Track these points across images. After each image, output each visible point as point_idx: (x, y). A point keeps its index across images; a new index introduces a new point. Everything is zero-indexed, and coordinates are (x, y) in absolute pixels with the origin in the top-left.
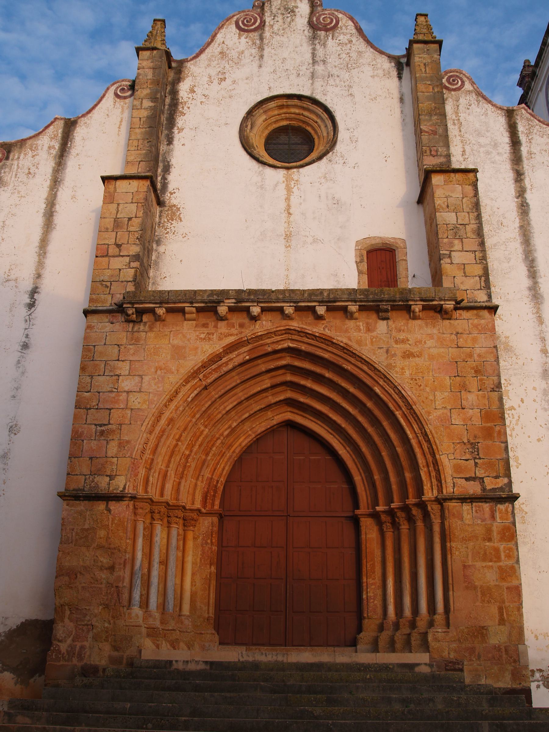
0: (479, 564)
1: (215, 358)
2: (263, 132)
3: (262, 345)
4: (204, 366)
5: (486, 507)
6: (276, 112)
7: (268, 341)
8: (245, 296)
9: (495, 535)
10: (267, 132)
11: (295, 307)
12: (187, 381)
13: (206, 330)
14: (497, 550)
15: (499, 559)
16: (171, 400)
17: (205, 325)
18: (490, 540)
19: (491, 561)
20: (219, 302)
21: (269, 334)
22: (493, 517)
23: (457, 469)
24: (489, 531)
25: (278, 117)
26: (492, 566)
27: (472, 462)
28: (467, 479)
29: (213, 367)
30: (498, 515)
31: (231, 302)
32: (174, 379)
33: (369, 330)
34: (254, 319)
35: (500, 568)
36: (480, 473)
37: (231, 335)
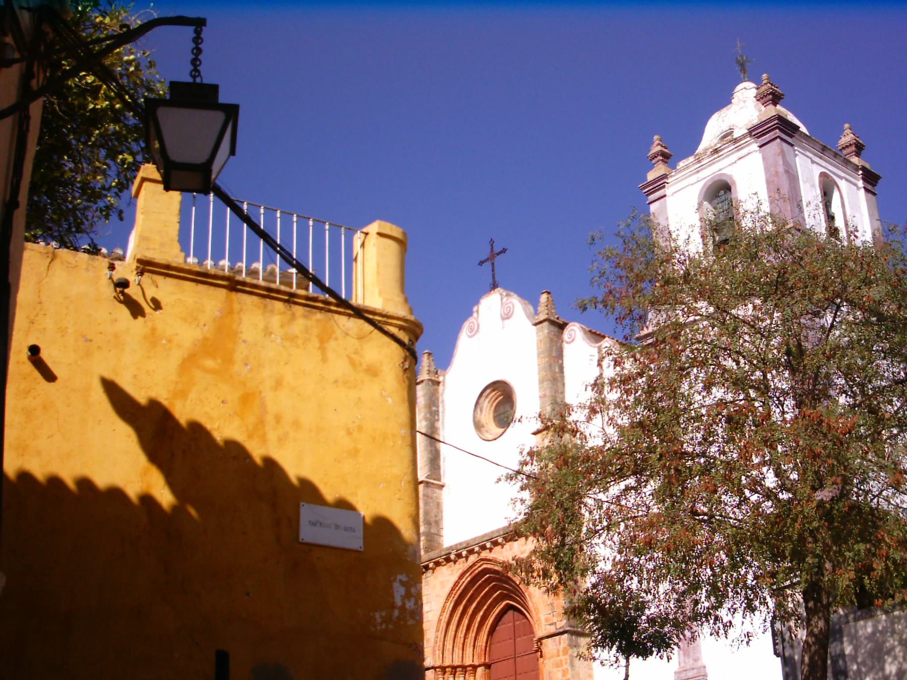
0: (555, 670)
1: (456, 584)
2: (490, 410)
3: (475, 570)
4: (452, 589)
5: (557, 637)
6: (493, 394)
7: (476, 567)
8: (459, 547)
9: (561, 653)
10: (493, 408)
11: (479, 546)
12: (447, 599)
13: (451, 569)
14: (561, 661)
15: (562, 664)
16: (443, 612)
17: (450, 566)
18: (559, 656)
19: (559, 667)
20: (450, 553)
21: (474, 565)
22: (560, 643)
23: (547, 620)
24: (558, 651)
25: (496, 396)
26: (559, 671)
27: (552, 615)
28: (550, 625)
29: (457, 588)
30: (562, 642)
31: (454, 552)
32: (443, 600)
33: (511, 549)
34: (467, 557)
35: (563, 670)
36: (555, 620)
37: (461, 569)
